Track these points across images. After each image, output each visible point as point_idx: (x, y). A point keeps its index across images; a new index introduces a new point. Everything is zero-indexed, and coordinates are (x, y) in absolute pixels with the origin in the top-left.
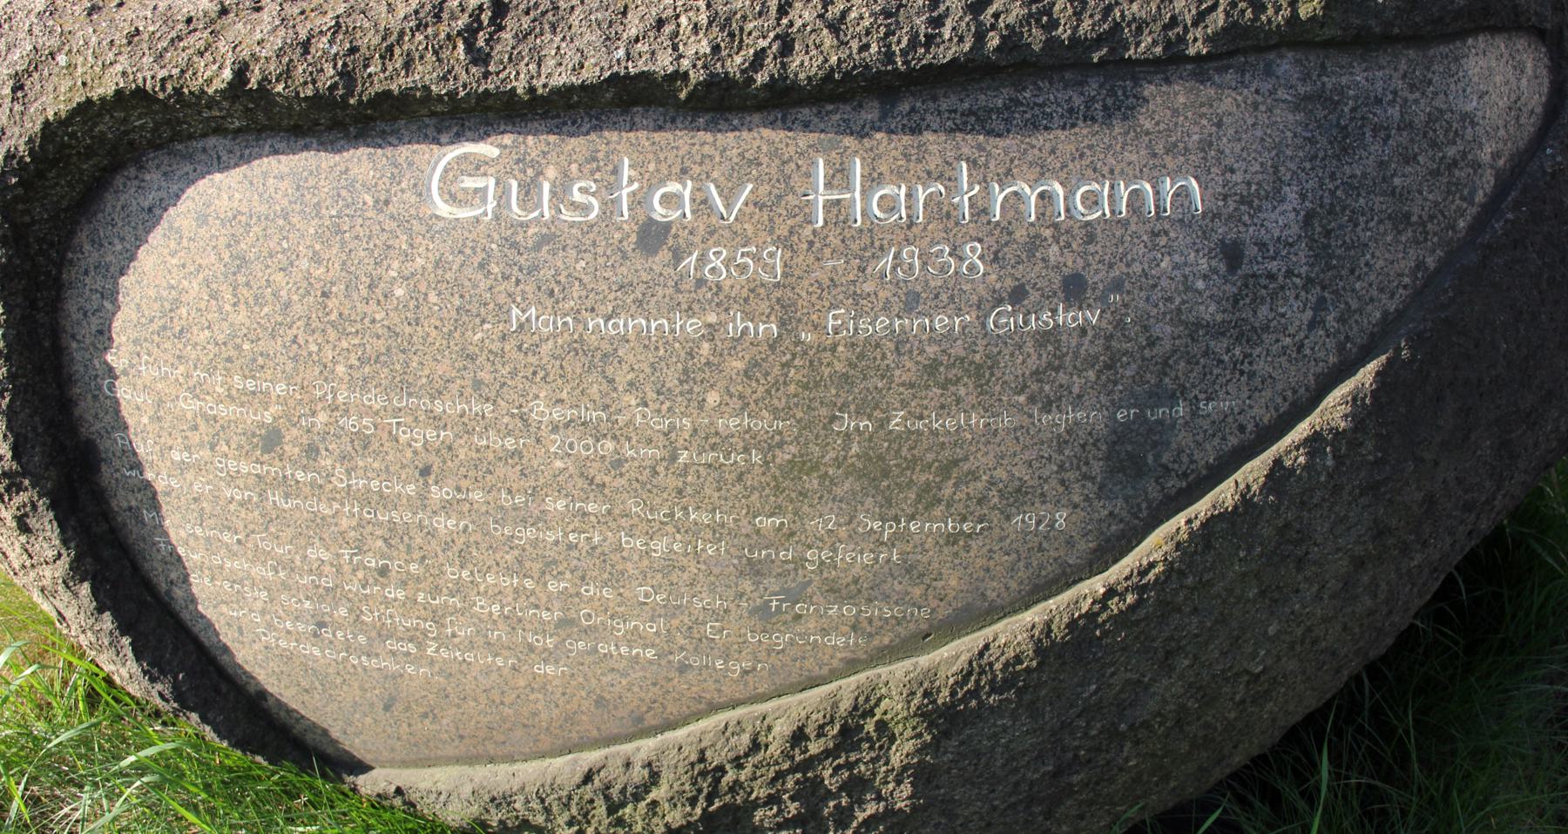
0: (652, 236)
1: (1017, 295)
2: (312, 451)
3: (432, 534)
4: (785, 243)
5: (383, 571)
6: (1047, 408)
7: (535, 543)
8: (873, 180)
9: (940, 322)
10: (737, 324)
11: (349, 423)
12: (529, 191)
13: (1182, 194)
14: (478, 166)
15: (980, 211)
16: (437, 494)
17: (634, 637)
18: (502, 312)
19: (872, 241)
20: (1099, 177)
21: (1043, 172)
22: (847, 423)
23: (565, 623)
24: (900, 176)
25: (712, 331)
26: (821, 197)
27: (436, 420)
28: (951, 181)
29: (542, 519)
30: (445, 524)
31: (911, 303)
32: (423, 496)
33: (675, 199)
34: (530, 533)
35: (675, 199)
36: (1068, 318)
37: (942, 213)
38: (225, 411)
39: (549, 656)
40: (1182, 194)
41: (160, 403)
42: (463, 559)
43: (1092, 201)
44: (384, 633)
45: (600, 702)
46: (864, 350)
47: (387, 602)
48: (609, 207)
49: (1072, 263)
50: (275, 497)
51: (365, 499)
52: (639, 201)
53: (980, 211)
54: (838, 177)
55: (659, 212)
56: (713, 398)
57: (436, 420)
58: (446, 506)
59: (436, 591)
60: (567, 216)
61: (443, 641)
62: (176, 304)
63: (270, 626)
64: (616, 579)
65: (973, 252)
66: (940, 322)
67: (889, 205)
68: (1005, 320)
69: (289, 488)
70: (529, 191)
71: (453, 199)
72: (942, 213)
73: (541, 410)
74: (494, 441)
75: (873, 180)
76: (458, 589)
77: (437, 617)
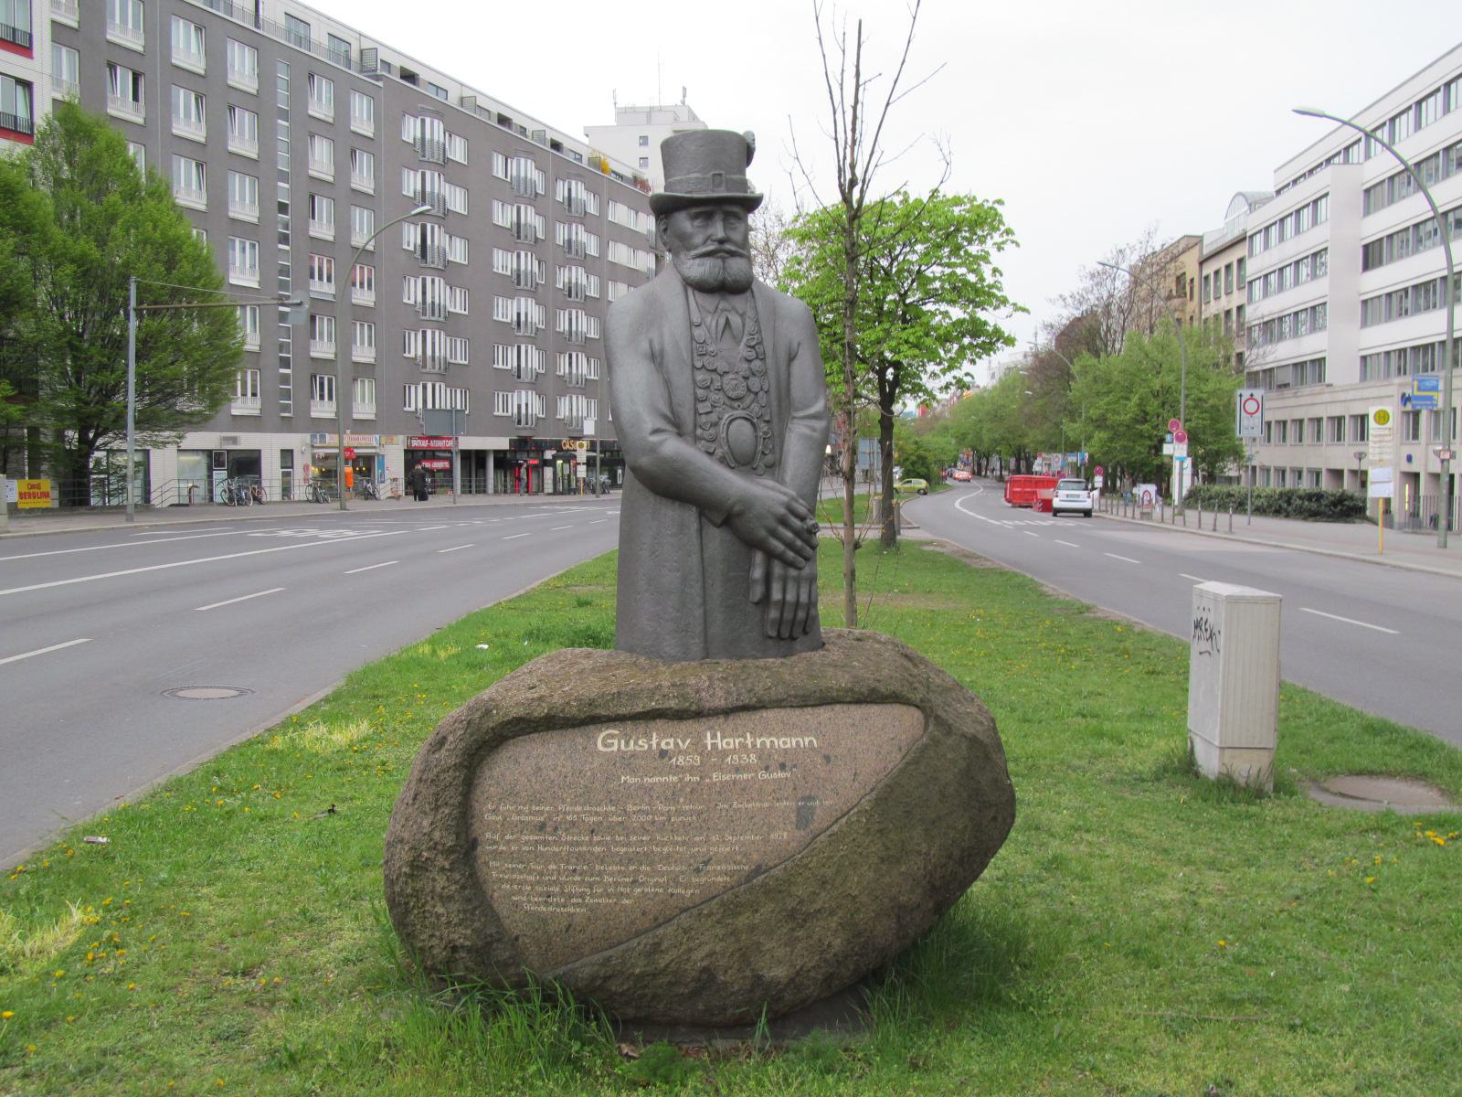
0: (663, 754)
1: (767, 768)
2: (556, 829)
3: (593, 853)
4: (701, 754)
5: (574, 871)
6: (778, 800)
7: (626, 853)
8: (723, 737)
9: (745, 776)
10: (688, 778)
11: (568, 818)
12: (627, 744)
13: (811, 742)
14: (612, 736)
15: (754, 745)
16: (596, 839)
17: (657, 885)
18: (619, 778)
19: (725, 753)
20: (786, 736)
21: (771, 735)
22: (721, 806)
23: (634, 882)
24: (731, 736)
25: (681, 780)
26: (709, 742)
27: (597, 814)
28: (745, 738)
29: (628, 844)
30: (597, 849)
31: (737, 770)
32: (591, 840)
33: (668, 744)
34: (624, 850)
35: (668, 744)
36: (781, 775)
37: (743, 746)
38: (527, 819)
39: (628, 896)
40: (811, 742)
41: (505, 819)
42: (602, 862)
43: (785, 743)
44: (571, 896)
45: (644, 914)
46: (724, 784)
47: (574, 883)
48: (650, 746)
49: (781, 760)
50: (541, 848)
51: (571, 844)
52: (658, 744)
53: (754, 745)
54: (714, 736)
55: (663, 746)
56: (682, 800)
57: (597, 814)
58: (599, 843)
59: (592, 876)
60: (638, 749)
61: (592, 896)
62: (516, 785)
63: (529, 902)
64: (651, 864)
65: (753, 756)
66: (745, 776)
67: (728, 744)
68: (763, 775)
69: (545, 843)
70: (627, 744)
71: (605, 745)
72: (743, 746)
73: (630, 808)
74: (615, 819)
75: (723, 737)
76: (600, 874)
77: (591, 886)
